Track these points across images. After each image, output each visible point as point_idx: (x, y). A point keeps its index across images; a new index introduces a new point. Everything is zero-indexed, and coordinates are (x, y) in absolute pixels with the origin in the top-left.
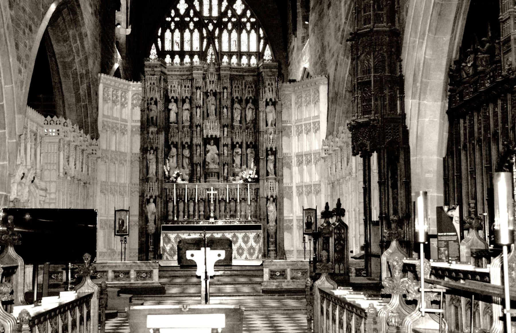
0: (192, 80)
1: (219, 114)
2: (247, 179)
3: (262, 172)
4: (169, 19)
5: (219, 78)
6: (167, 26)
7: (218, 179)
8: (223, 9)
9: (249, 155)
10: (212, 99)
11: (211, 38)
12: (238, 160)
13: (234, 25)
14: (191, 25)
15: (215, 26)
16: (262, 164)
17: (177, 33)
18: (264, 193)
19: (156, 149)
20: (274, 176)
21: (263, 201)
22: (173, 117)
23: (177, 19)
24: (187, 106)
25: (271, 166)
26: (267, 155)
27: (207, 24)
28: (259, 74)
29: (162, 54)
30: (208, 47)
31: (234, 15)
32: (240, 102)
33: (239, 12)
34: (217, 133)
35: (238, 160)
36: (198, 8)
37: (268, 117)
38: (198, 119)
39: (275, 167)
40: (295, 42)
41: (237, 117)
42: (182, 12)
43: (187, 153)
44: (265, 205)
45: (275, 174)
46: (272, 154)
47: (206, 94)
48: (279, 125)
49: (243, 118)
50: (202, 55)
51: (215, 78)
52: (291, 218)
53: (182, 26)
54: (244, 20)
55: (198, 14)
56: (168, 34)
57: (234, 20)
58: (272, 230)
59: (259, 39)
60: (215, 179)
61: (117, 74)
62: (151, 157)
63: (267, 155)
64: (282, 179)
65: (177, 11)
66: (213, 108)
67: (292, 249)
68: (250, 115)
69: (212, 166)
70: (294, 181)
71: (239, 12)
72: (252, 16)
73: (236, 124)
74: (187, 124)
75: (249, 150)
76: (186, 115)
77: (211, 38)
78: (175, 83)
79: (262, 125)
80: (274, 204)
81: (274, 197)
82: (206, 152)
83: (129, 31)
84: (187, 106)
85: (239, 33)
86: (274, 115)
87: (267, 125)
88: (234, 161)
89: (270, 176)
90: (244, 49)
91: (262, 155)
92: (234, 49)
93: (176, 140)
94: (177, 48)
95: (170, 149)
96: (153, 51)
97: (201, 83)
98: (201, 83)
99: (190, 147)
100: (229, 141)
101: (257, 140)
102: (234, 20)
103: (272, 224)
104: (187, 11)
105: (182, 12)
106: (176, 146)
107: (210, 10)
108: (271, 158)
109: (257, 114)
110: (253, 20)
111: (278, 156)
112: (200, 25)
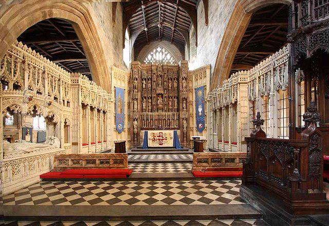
0: (152, 71)
1: (163, 84)
3: (181, 108)
4: (145, 61)
5: (163, 70)
8: (163, 58)
12: (170, 104)
16: (181, 104)
19: (137, 99)
23: (148, 61)
24: (150, 81)
26: (183, 100)
28: (179, 68)
32: (171, 79)
33: (168, 58)
34: (162, 92)
35: (170, 104)
38: (154, 87)
39: (186, 105)
41: (170, 86)
42: (150, 59)
43: (150, 101)
47: (157, 76)
48: (188, 88)
49: (173, 85)
51: (161, 70)
62: (135, 102)
63: (183, 100)
66: (160, 82)
68: (175, 85)
76: (150, 85)
79: (181, 88)
82: (157, 100)
83: (131, 62)
84: (150, 81)
91: (181, 101)
93: (145, 95)
95: (143, 99)
97: (155, 72)
98: (155, 72)
99: (151, 98)
101: (178, 95)
103: (185, 129)
104: (151, 59)
105: (150, 59)
106: (145, 98)
110: (173, 61)
111: (188, 101)
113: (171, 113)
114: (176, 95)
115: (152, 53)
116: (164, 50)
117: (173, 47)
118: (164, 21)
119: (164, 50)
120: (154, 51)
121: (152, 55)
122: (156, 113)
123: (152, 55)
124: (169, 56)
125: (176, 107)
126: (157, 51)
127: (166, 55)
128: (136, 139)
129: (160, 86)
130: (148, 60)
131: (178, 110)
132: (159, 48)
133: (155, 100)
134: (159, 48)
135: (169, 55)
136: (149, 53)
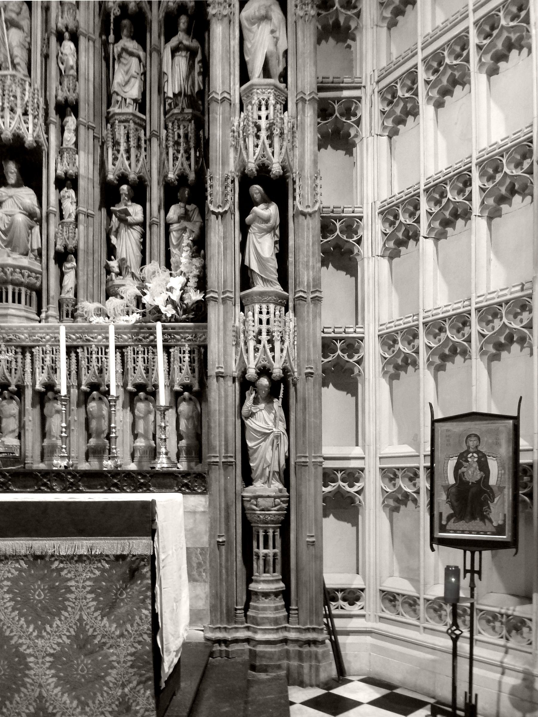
2: (157, 309)
7: (39, 313)
9: (175, 227)
20: (278, 288)
37: (248, 45)
44: (231, 411)
45: (283, 279)
46: (267, 200)
52: (353, 464)
64: (317, 300)
67: (357, 583)
70: (369, 316)
80: (277, 404)
81: (277, 372)
86: (281, 33)
87: (244, 77)
88: (111, 251)
89: (259, 287)
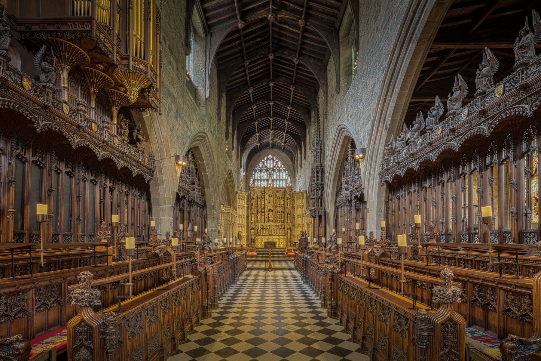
1: (273, 202)
3: (286, 220)
4: (256, 169)
6: (256, 171)
8: (274, 165)
10: (271, 197)
11: (270, 175)
13: (278, 170)
14: (264, 171)
15: (272, 171)
16: (286, 218)
17: (259, 173)
18: (286, 227)
19: (254, 214)
21: (286, 229)
22: (259, 203)
23: (259, 169)
24: (263, 200)
25: (289, 218)
27: (269, 170)
28: (285, 190)
29: (254, 180)
30: (269, 178)
31: (278, 167)
32: (279, 198)
33: (279, 166)
34: (272, 208)
36: (266, 165)
38: (266, 204)
40: (297, 177)
42: (261, 166)
43: (263, 214)
49: (280, 203)
50: (268, 180)
51: (272, 191)
53: (261, 171)
54: (281, 168)
55: (266, 167)
56: (256, 174)
57: (278, 168)
58: (289, 238)
59: (286, 175)
60: (272, 222)
61: (241, 190)
62: (253, 216)
65: (259, 166)
68: (282, 202)
69: (271, 218)
71: (279, 166)
72: (284, 167)
73: (278, 205)
74: (263, 205)
75: (282, 213)
76: (263, 202)
77: (270, 175)
78: (259, 192)
79: (286, 205)
82: (269, 214)
84: (263, 200)
85: (280, 173)
90: (281, 178)
92: (278, 178)
94: (259, 178)
96: (252, 179)
98: (267, 192)
99: (264, 212)
100: (276, 210)
102: (278, 168)
103: (289, 236)
105: (261, 166)
107: (270, 165)
108: (289, 216)
109: (284, 202)
110: (284, 168)
112: (267, 170)
113: (279, 224)
114: (283, 210)
115: (263, 161)
116: (274, 158)
117: (284, 155)
118: (274, 137)
119: (274, 158)
120: (266, 158)
121: (263, 162)
122: (268, 224)
123: (263, 162)
124: (279, 164)
125: (283, 220)
126: (268, 159)
127: (277, 162)
128: (253, 243)
129: (271, 203)
130: (259, 167)
131: (284, 222)
132: (270, 155)
133: (266, 214)
134: (270, 155)
135: (279, 163)
136: (261, 161)
